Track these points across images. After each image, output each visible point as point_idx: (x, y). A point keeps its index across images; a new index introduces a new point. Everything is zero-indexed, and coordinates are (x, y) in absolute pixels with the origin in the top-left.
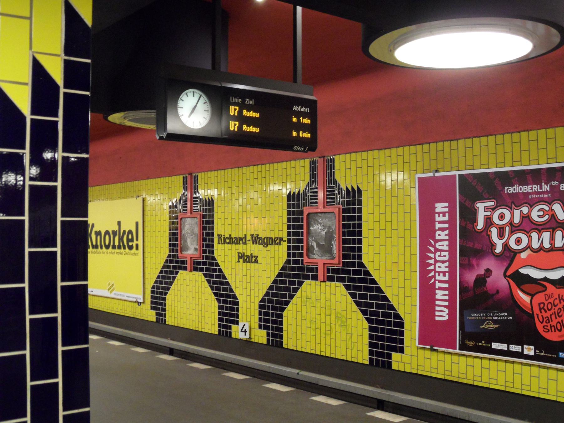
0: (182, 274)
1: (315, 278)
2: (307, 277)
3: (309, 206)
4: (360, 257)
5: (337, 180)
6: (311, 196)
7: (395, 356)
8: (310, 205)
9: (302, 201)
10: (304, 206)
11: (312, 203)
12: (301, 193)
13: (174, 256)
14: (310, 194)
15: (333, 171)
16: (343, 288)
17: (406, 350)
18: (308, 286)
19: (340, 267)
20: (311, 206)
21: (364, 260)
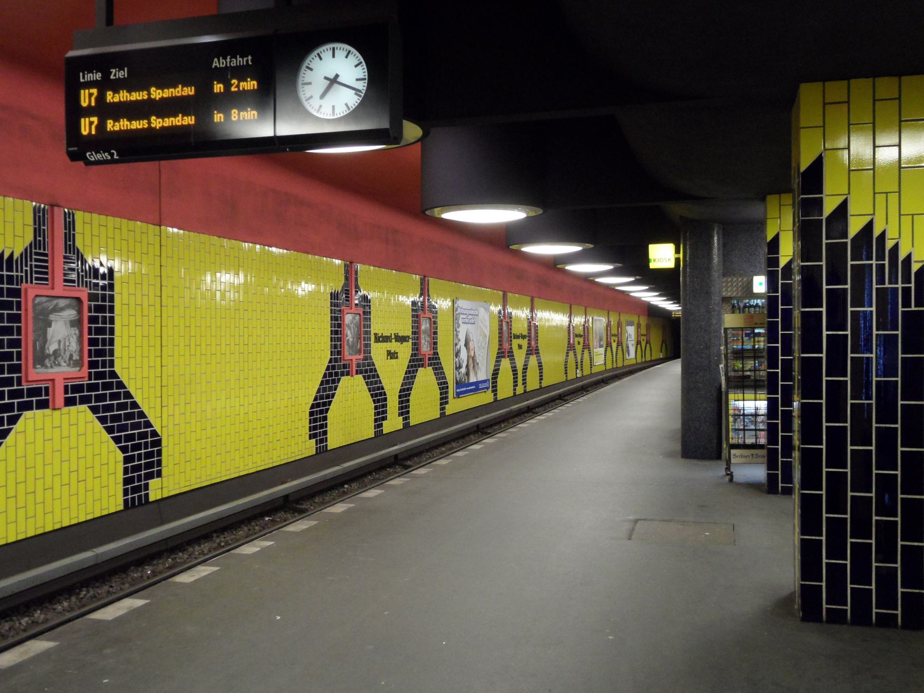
0: (345, 380)
1: (43, 405)
2: (27, 406)
3: (31, 282)
4: (112, 363)
5: (79, 247)
6: (36, 266)
7: (154, 483)
8: (34, 282)
9: (17, 271)
10: (22, 282)
11: (37, 279)
12: (15, 257)
13: (336, 360)
14: (34, 263)
15: (72, 232)
16: (89, 412)
17: (164, 472)
18: (30, 423)
19: (84, 381)
20: (36, 283)
21: (117, 369)
